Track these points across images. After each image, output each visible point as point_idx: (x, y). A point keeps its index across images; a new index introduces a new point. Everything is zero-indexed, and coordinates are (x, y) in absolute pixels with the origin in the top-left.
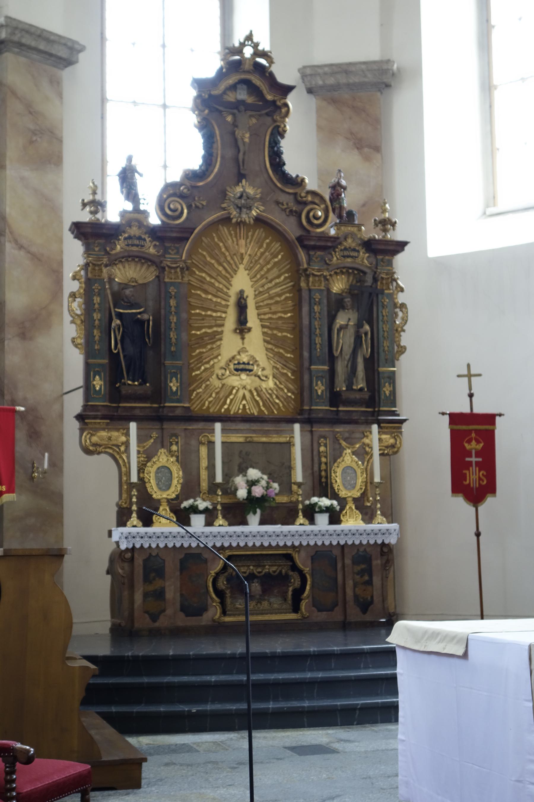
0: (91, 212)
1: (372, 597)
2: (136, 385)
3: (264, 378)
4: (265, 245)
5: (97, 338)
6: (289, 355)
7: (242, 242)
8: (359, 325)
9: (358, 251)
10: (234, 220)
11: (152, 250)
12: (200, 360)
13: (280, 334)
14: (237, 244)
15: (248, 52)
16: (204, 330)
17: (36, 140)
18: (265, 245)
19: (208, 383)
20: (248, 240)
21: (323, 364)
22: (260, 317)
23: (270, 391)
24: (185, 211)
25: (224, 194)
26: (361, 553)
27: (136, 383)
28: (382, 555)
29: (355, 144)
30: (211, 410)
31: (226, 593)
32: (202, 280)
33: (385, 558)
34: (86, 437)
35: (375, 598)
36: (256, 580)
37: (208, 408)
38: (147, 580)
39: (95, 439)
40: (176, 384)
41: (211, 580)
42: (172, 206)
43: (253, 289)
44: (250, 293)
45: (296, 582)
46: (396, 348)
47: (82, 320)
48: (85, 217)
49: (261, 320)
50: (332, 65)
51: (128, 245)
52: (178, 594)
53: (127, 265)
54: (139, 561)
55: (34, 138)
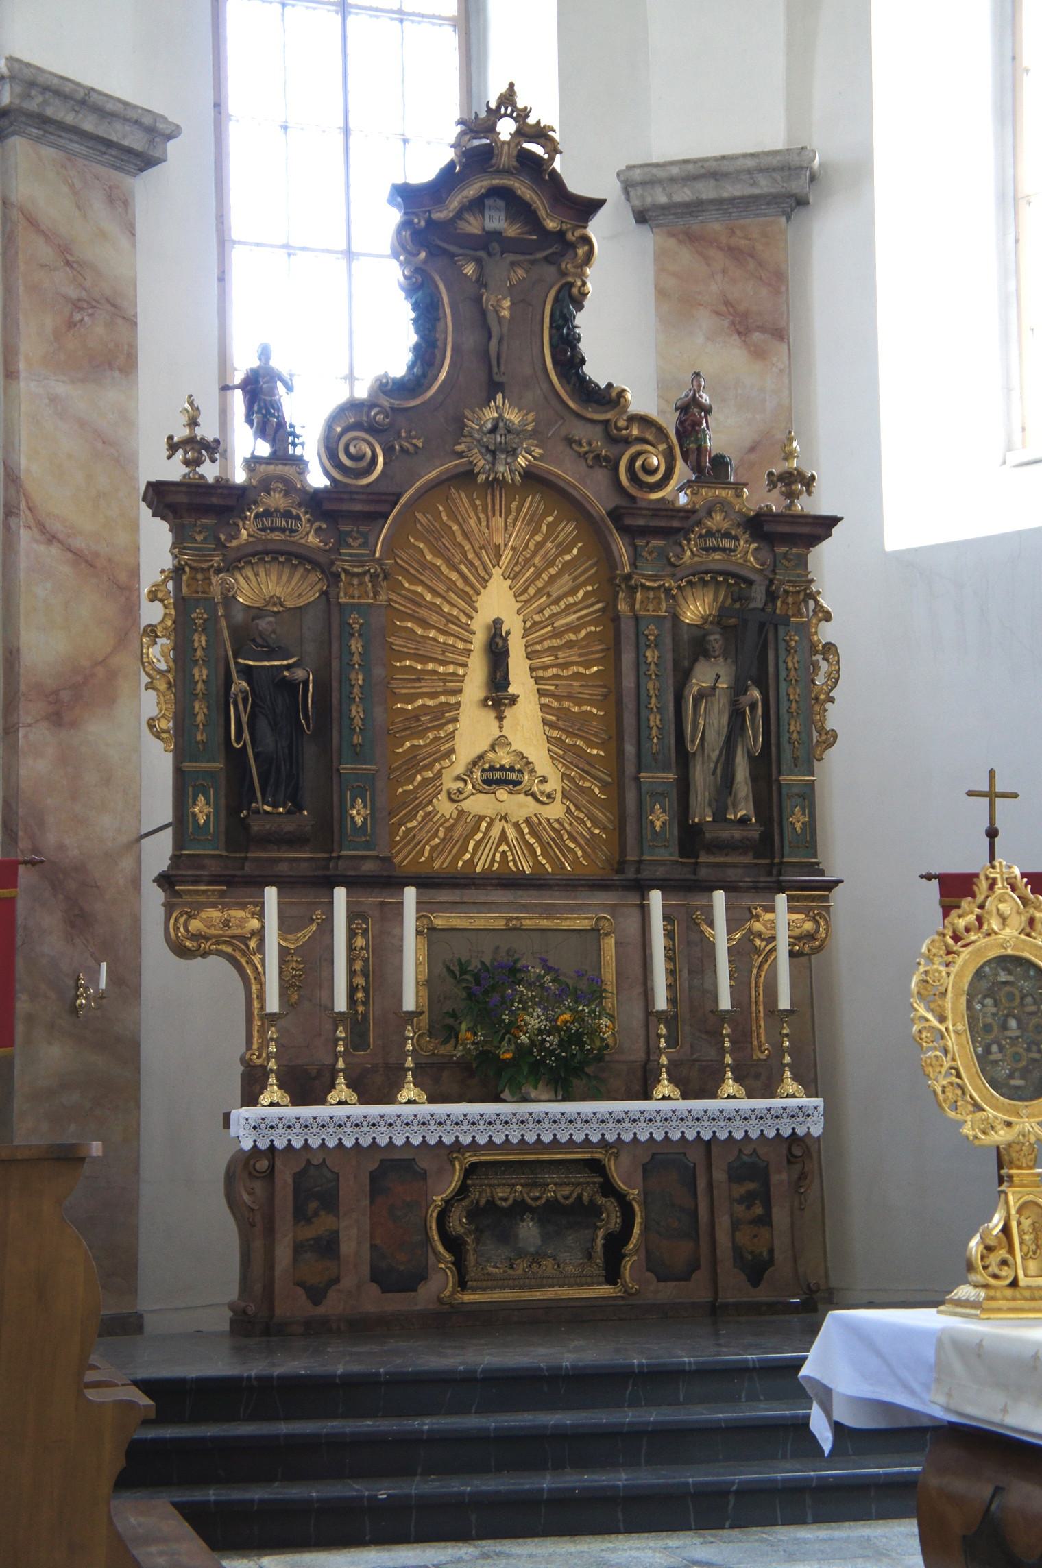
0: (187, 463)
1: (771, 1251)
2: (281, 813)
3: (545, 799)
4: (544, 528)
5: (200, 718)
6: (595, 752)
7: (498, 522)
8: (738, 689)
9: (736, 538)
10: (481, 478)
11: (313, 540)
12: (413, 762)
13: (576, 709)
14: (488, 527)
15: (506, 128)
16: (420, 702)
17: (82, 320)
18: (544, 528)
19: (430, 808)
20: (510, 520)
21: (665, 769)
22: (534, 674)
23: (556, 825)
24: (381, 459)
25: (459, 427)
26: (745, 1158)
27: (281, 810)
28: (789, 1162)
29: (733, 323)
30: (436, 865)
31: (466, 1243)
32: (417, 600)
33: (798, 1167)
34: (176, 920)
36: (527, 1216)
37: (431, 859)
38: (300, 1215)
39: (195, 925)
40: (362, 812)
41: (435, 1215)
42: (352, 450)
43: (521, 617)
44: (514, 625)
45: (614, 1220)
46: (815, 734)
47: (169, 683)
48: (174, 470)
49: (537, 680)
50: (686, 162)
51: (263, 529)
52: (368, 1245)
53: (262, 573)
54: (285, 1176)
55: (77, 317)
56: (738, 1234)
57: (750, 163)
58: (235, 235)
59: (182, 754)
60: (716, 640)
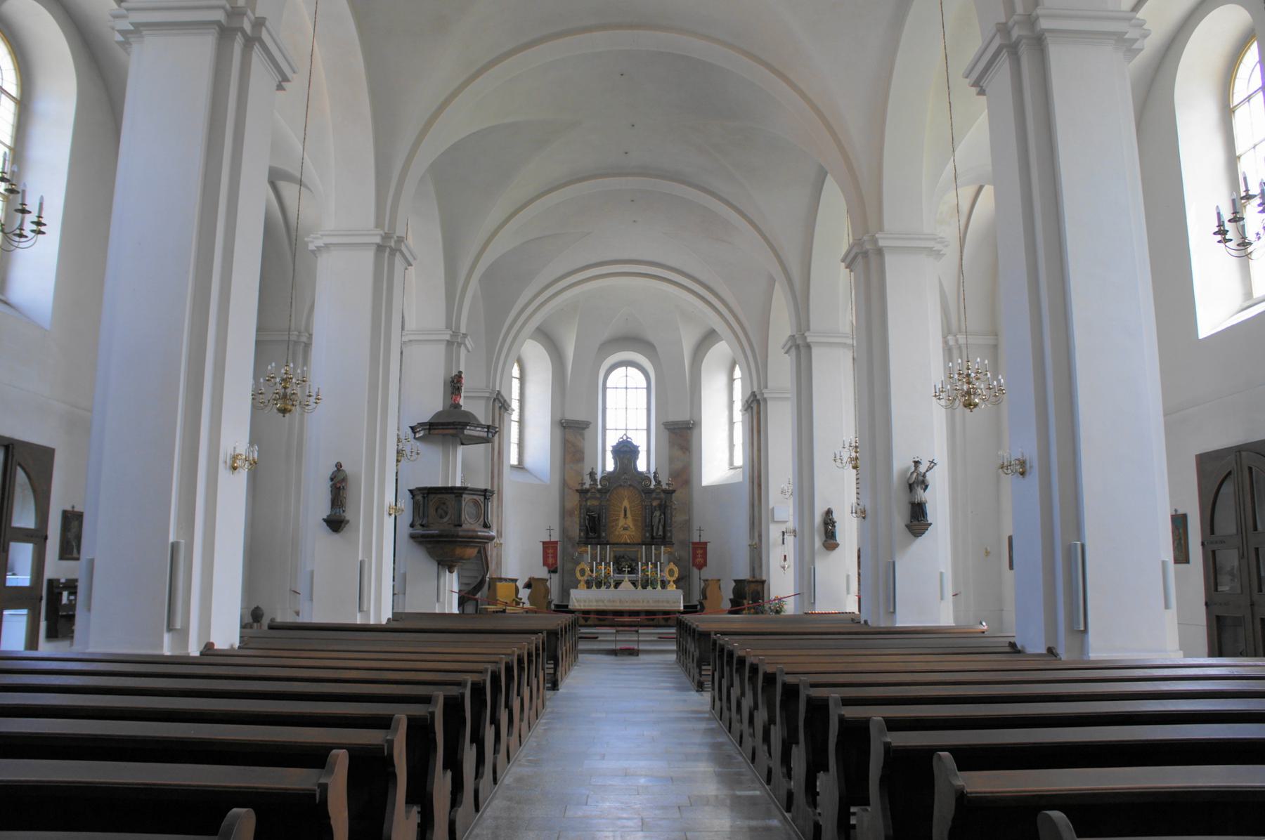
8: (660, 515)
12: (613, 527)
48: (579, 488)
58: (607, 428)
59: (581, 526)
60: (657, 509)
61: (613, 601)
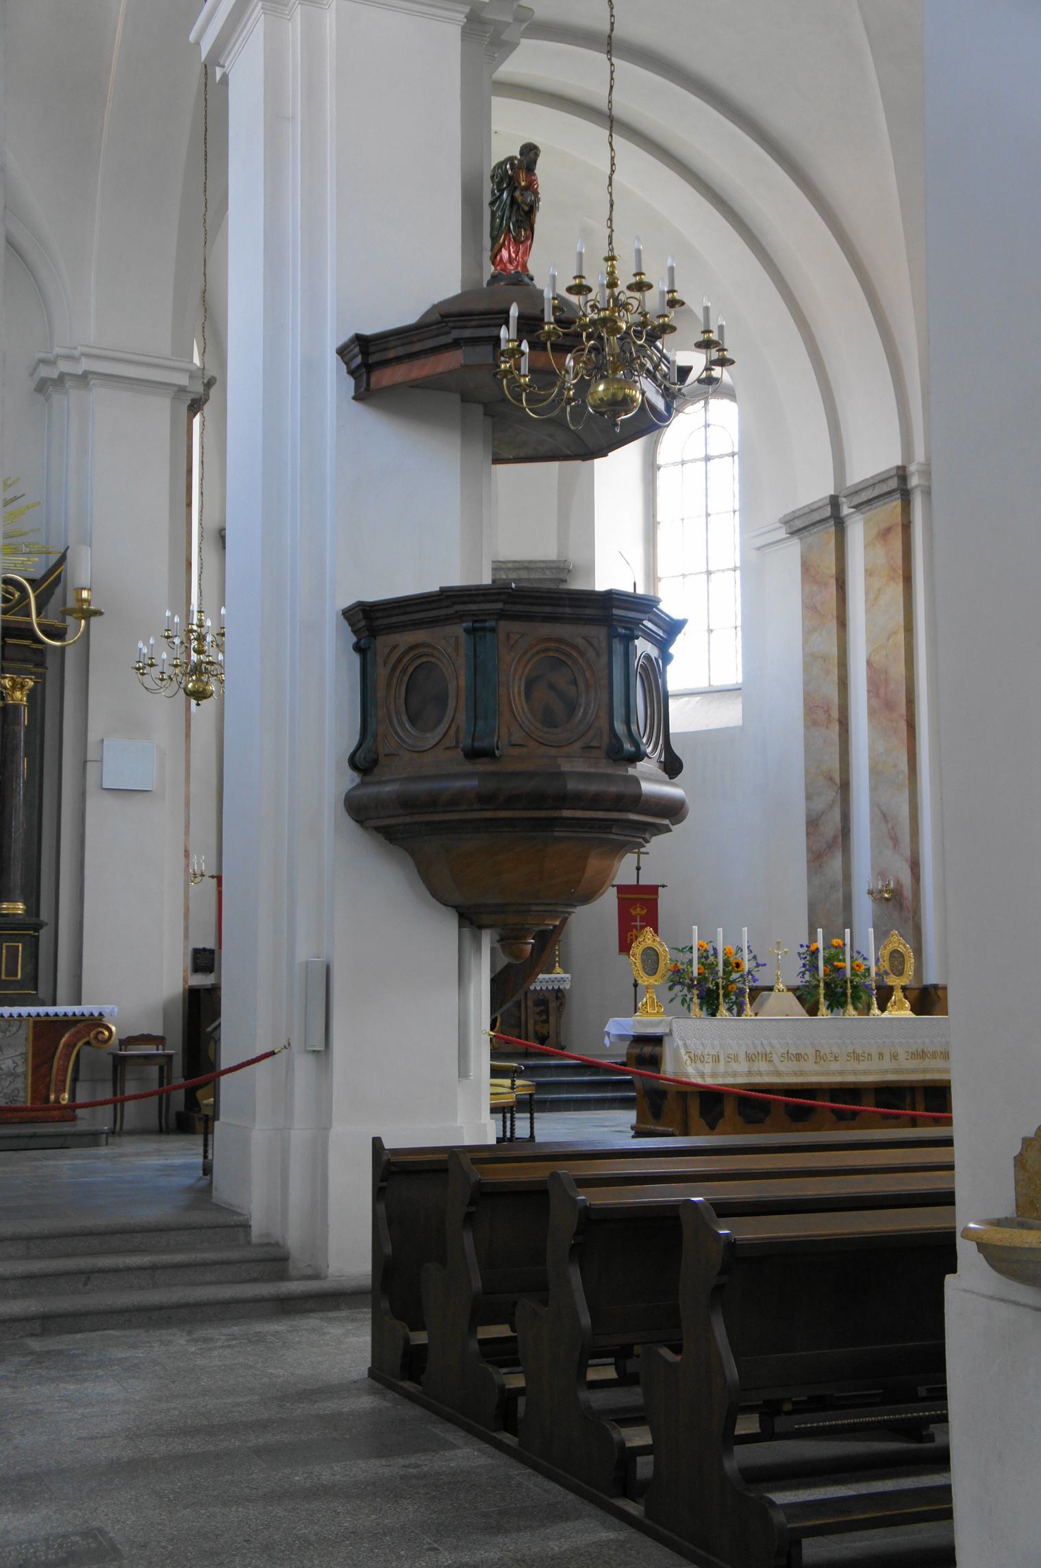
1: (548, 1033)
26: (540, 997)
28: (557, 999)
33: (559, 1001)
35: (550, 1033)
50: (515, 562)
56: (536, 1026)
57: (543, 565)
61: (798, 1057)
